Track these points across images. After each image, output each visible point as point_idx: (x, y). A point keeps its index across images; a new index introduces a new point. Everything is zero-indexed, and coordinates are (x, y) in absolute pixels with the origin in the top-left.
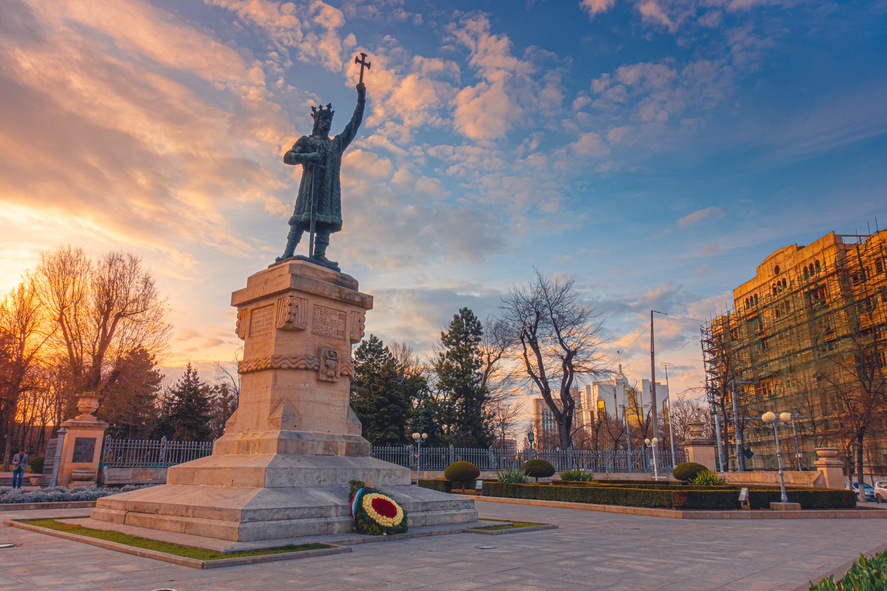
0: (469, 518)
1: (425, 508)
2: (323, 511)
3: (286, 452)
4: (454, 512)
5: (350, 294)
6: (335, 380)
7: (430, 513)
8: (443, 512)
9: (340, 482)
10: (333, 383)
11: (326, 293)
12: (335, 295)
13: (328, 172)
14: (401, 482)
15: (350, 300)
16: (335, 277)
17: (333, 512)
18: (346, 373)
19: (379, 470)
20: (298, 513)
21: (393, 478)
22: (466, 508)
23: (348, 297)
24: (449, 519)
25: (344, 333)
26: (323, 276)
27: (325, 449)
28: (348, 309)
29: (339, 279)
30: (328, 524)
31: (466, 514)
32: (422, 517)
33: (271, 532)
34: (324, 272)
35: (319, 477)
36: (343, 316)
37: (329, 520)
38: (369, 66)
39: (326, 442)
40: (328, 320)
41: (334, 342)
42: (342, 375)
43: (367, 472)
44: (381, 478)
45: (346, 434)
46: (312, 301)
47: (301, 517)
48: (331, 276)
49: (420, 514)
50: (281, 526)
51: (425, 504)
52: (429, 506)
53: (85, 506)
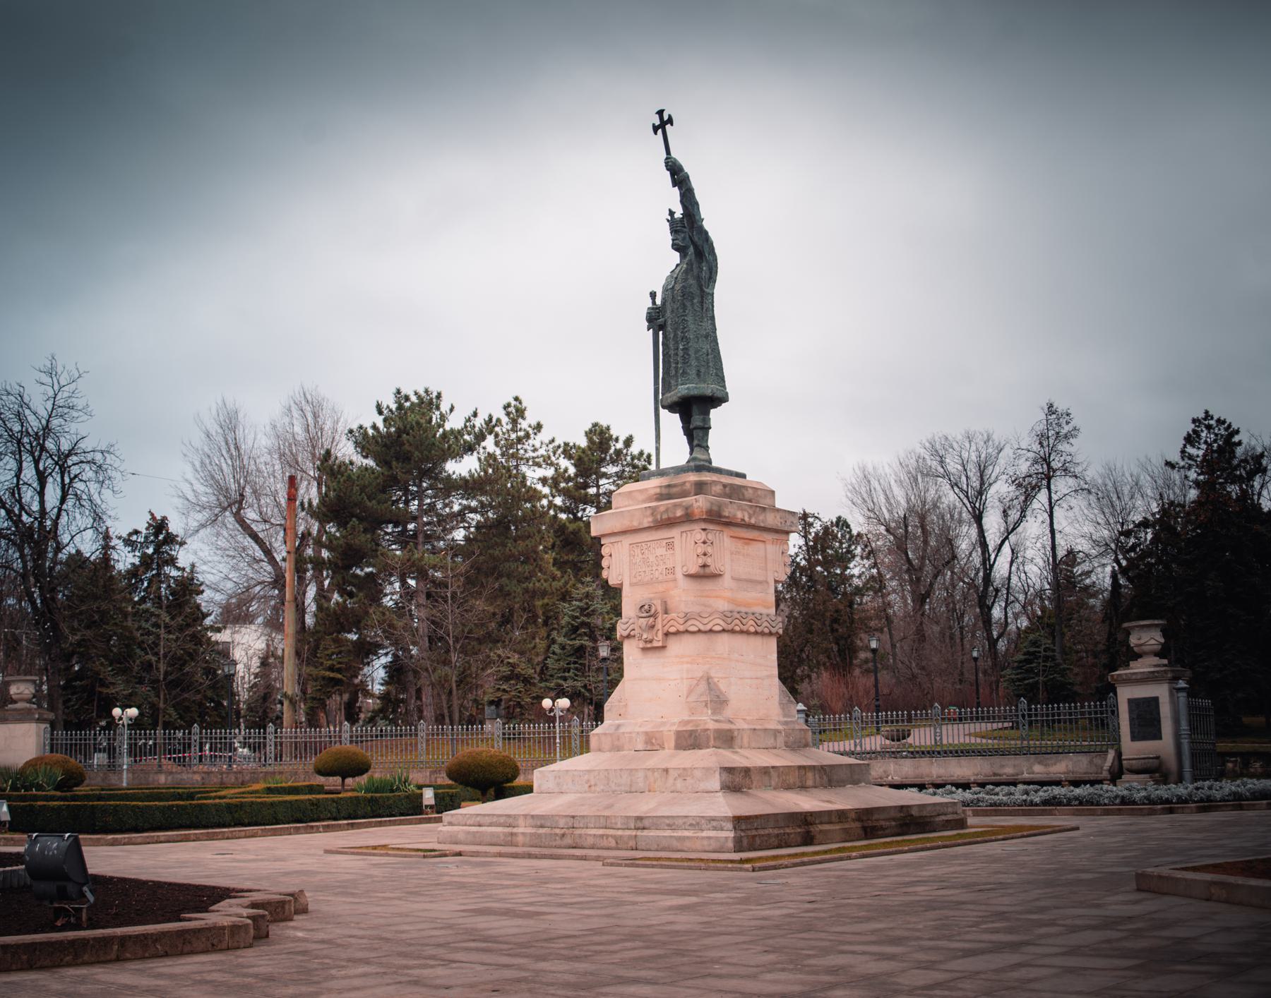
0: (714, 845)
1: (639, 824)
2: (511, 820)
3: (600, 750)
4: (686, 833)
5: (667, 510)
6: (655, 644)
7: (645, 833)
8: (668, 833)
9: (614, 788)
10: (664, 647)
11: (635, 524)
12: (647, 522)
13: (669, 322)
14: (704, 785)
15: (669, 519)
16: (658, 491)
17: (521, 822)
18: (672, 630)
19: (666, 770)
20: (488, 820)
21: (690, 781)
22: (715, 829)
23: (665, 516)
24: (675, 844)
25: (672, 571)
26: (641, 497)
27: (646, 743)
28: (675, 533)
29: (664, 491)
30: (512, 834)
31: (709, 838)
32: (630, 837)
33: (461, 837)
34: (640, 491)
35: (588, 781)
36: (670, 546)
37: (515, 830)
38: (670, 121)
39: (646, 733)
40: (652, 559)
41: (660, 588)
42: (667, 634)
43: (650, 773)
44: (671, 781)
45: (686, 718)
46: (627, 541)
47: (490, 825)
48: (652, 492)
49: (628, 833)
50: (469, 833)
51: (640, 818)
52: (646, 823)
53: (1050, 813)
